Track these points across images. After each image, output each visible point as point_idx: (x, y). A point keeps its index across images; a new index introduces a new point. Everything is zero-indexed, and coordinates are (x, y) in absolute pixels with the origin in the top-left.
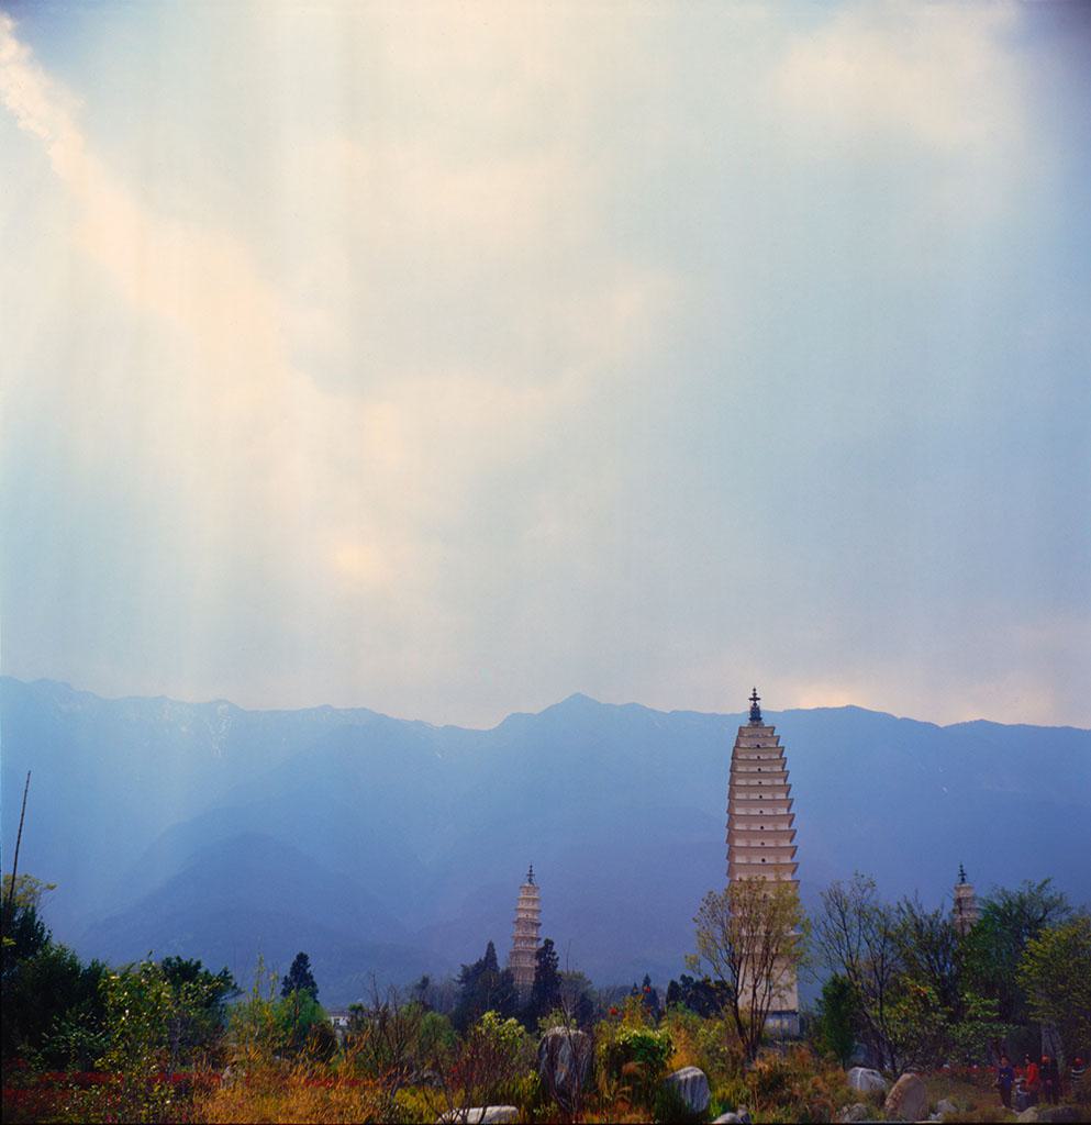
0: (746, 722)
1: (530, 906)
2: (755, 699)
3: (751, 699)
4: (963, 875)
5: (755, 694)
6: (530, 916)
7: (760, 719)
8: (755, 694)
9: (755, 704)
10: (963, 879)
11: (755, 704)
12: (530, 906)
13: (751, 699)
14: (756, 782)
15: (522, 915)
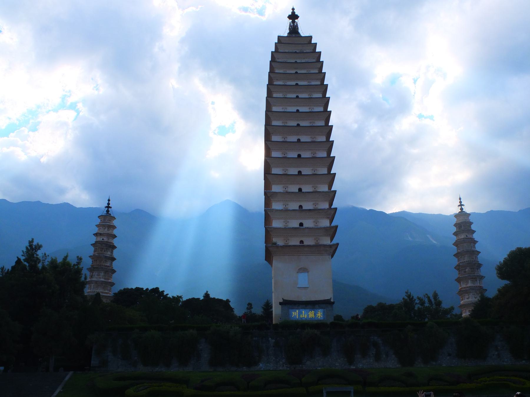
0: (285, 32)
1: (106, 231)
2: (293, 17)
3: (290, 17)
4: (461, 205)
5: (293, 13)
6: (106, 239)
7: (299, 33)
8: (293, 13)
9: (293, 22)
10: (462, 209)
11: (293, 22)
12: (106, 231)
13: (290, 17)
14: (294, 83)
15: (100, 239)
